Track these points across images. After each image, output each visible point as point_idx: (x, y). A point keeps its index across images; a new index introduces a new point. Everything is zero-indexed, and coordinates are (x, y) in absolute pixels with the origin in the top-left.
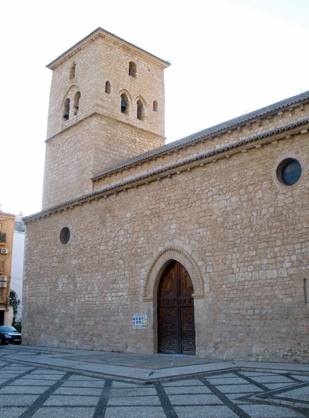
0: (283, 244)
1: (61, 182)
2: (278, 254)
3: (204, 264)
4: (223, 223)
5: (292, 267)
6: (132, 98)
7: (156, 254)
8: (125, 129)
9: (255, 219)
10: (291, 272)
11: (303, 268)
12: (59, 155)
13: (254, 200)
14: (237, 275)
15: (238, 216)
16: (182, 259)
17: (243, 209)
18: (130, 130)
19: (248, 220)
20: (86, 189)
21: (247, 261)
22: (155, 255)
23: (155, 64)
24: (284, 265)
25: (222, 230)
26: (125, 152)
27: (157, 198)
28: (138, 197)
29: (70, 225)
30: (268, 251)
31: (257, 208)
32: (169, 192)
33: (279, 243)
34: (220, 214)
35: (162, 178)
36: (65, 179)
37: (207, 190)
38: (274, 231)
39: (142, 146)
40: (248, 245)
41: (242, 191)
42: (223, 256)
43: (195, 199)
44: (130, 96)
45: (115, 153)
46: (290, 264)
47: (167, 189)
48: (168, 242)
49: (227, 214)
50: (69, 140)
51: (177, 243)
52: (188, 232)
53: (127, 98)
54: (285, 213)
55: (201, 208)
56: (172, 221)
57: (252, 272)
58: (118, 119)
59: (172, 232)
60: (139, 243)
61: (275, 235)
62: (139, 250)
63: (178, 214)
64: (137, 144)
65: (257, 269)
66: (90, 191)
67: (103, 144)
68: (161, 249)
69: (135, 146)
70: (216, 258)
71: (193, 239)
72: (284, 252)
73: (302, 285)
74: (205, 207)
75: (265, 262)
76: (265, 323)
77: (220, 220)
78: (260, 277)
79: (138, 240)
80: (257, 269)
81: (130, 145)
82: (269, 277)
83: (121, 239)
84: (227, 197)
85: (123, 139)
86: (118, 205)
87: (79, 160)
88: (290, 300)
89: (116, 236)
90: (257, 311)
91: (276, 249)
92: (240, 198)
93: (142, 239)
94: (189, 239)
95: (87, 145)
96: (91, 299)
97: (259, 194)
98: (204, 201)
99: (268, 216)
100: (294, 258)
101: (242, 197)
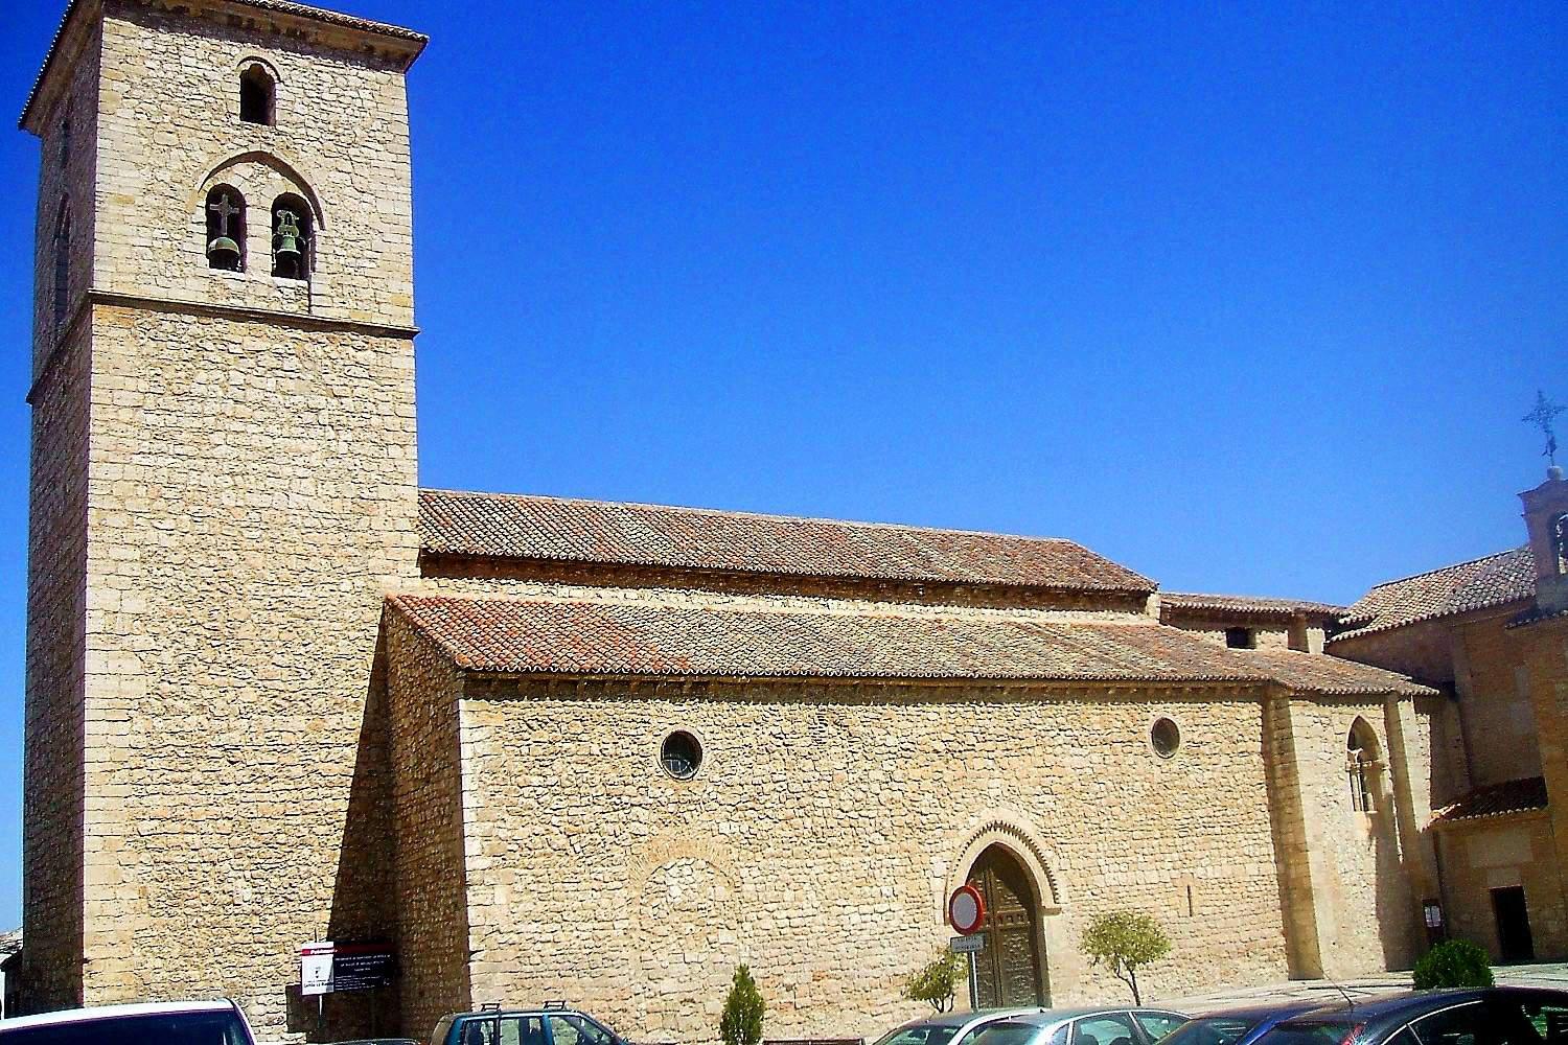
50: (268, 360)
51: (1007, 815)
63: (1004, 763)
83: (875, 788)
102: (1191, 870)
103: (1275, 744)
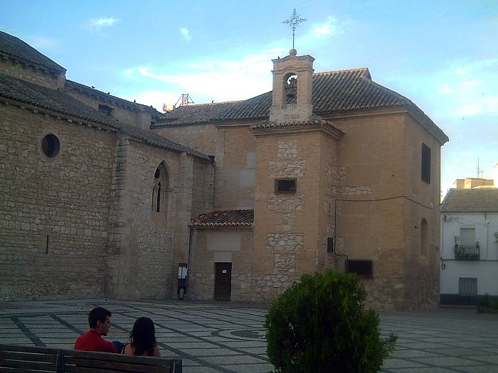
5: (41, 224)
13: (20, 156)
31: (22, 165)
38: (31, 190)
54: (42, 178)
76: (15, 268)
88: (37, 250)
90: (10, 257)
91: (31, 206)
97: (25, 153)
99: (29, 176)
100: (43, 217)
103: (115, 165)
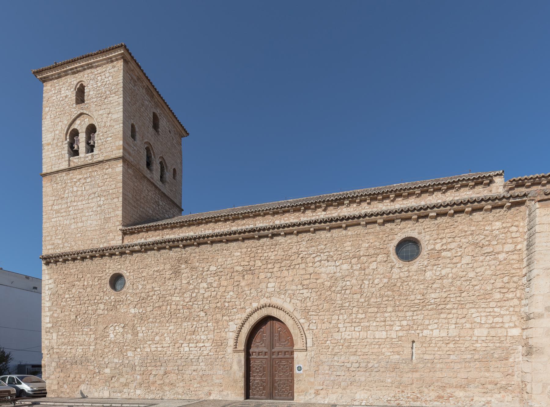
0: (394, 311)
1: (73, 227)
2: (388, 319)
3: (306, 321)
4: (330, 287)
6: (156, 156)
7: (250, 309)
8: (150, 188)
9: (366, 287)
10: (400, 334)
11: (413, 332)
12: (66, 195)
14: (343, 333)
15: (348, 282)
16: (282, 316)
17: (354, 276)
18: (154, 191)
19: (359, 287)
20: (113, 239)
21: (355, 322)
22: (248, 311)
23: (175, 127)
24: (394, 328)
25: (329, 293)
26: (151, 212)
27: (252, 255)
28: (225, 251)
29: (125, 272)
30: (378, 315)
32: (267, 251)
33: (390, 309)
34: (328, 279)
35: (260, 237)
36: (80, 225)
37: (314, 255)
39: (164, 211)
40: (357, 309)
41: (354, 261)
42: (329, 316)
43: (300, 262)
44: (154, 153)
45: (141, 209)
46: (400, 327)
47: (264, 248)
48: (265, 298)
49: (336, 279)
51: (275, 301)
52: (290, 292)
53: (151, 154)
55: (306, 270)
56: (270, 280)
57: (359, 332)
58: (145, 175)
59: (269, 290)
60: (227, 297)
61: (386, 302)
62: (227, 304)
63: (279, 274)
64: (160, 207)
65: (365, 330)
66: (118, 242)
67: (131, 196)
68: (255, 305)
69: (159, 208)
70: (321, 317)
71: (295, 298)
72: (395, 317)
73: (410, 345)
74: (311, 270)
75: (375, 324)
77: (328, 284)
78: (368, 336)
79: (226, 294)
80: (365, 330)
81: (154, 206)
82: (377, 337)
83: (202, 291)
84: (337, 264)
85: (149, 198)
86: (197, 258)
87: (100, 206)
89: (195, 288)
92: (352, 267)
93: (231, 293)
94: (290, 298)
95: (111, 191)
96: (159, 349)
98: (311, 264)
101: (354, 266)
102: (418, 332)
